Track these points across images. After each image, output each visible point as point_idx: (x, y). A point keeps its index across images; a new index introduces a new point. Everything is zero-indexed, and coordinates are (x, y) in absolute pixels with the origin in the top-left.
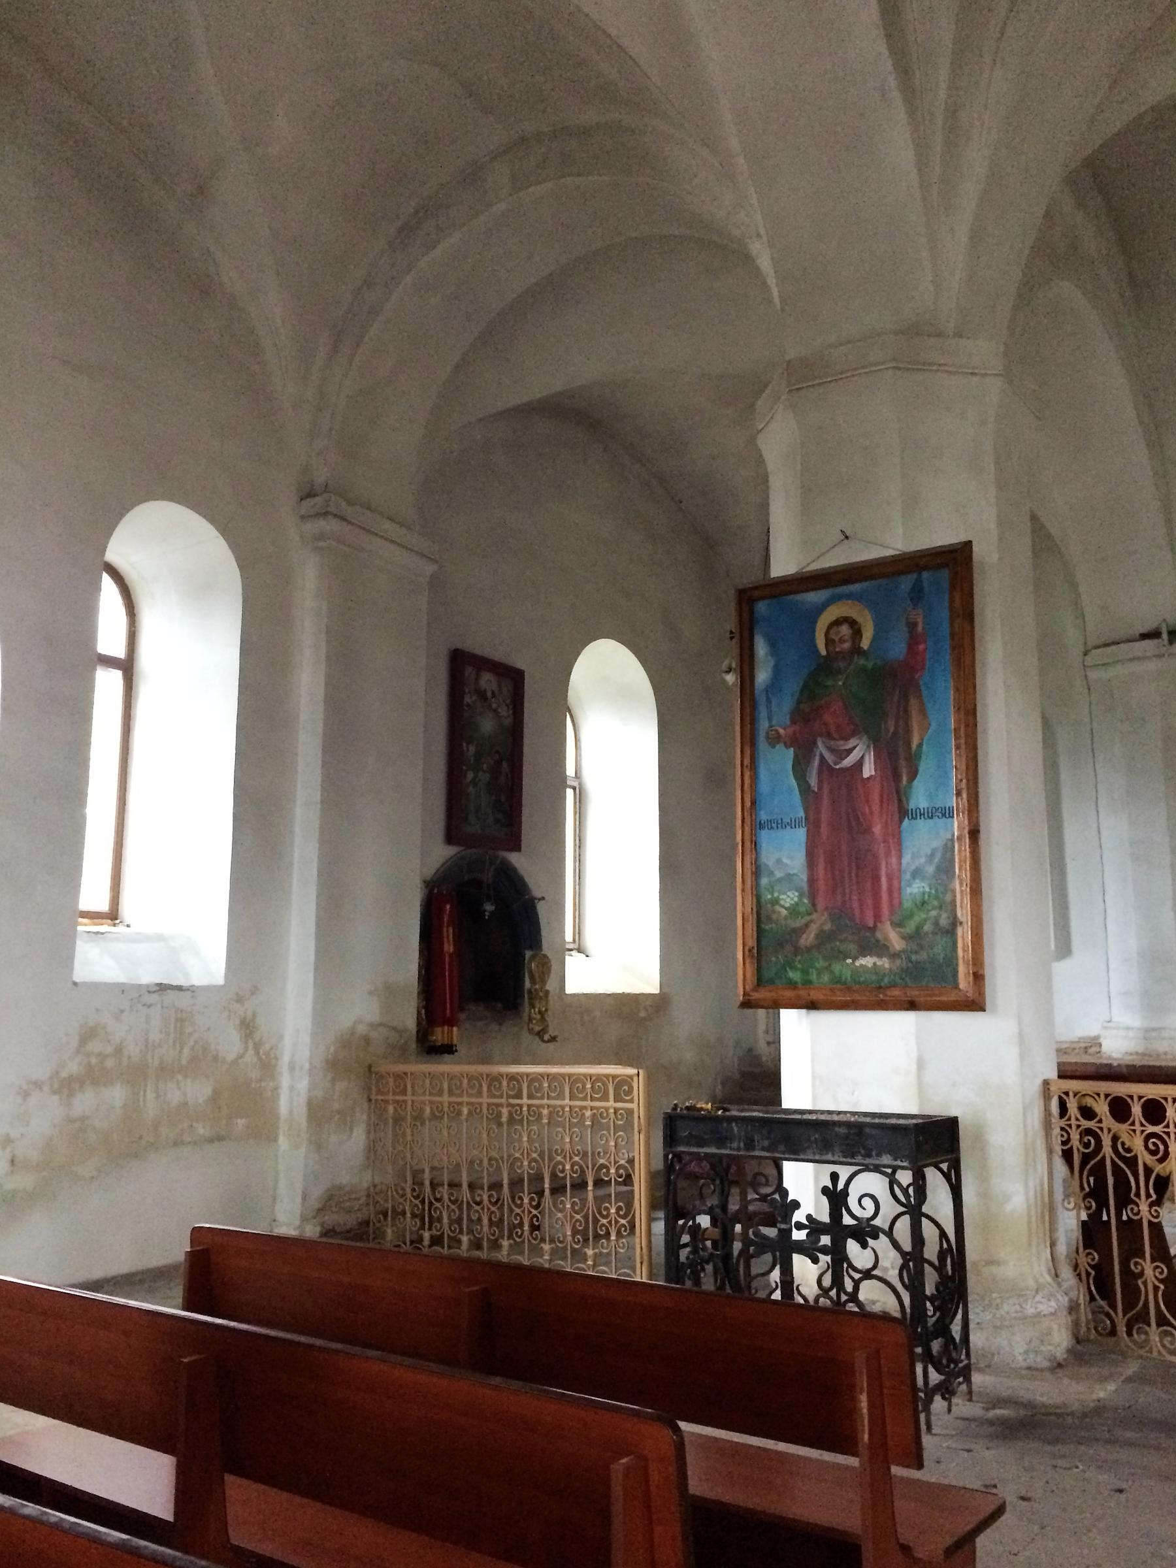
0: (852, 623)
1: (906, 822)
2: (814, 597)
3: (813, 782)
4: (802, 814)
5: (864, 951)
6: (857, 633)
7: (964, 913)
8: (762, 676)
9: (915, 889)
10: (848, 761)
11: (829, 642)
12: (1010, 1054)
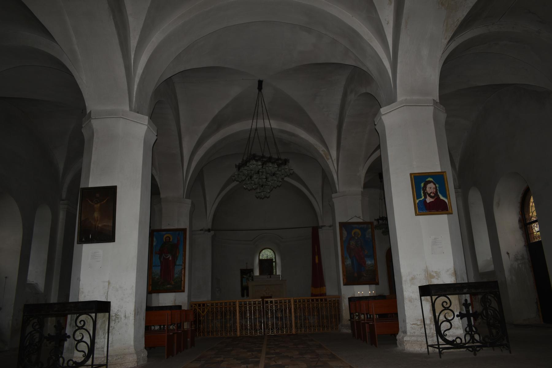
0: (169, 237)
1: (175, 266)
2: (164, 233)
3: (162, 260)
4: (160, 264)
5: (168, 285)
6: (170, 239)
7: (183, 279)
8: (154, 244)
9: (176, 276)
10: (168, 257)
11: (166, 240)
12: (186, 298)
